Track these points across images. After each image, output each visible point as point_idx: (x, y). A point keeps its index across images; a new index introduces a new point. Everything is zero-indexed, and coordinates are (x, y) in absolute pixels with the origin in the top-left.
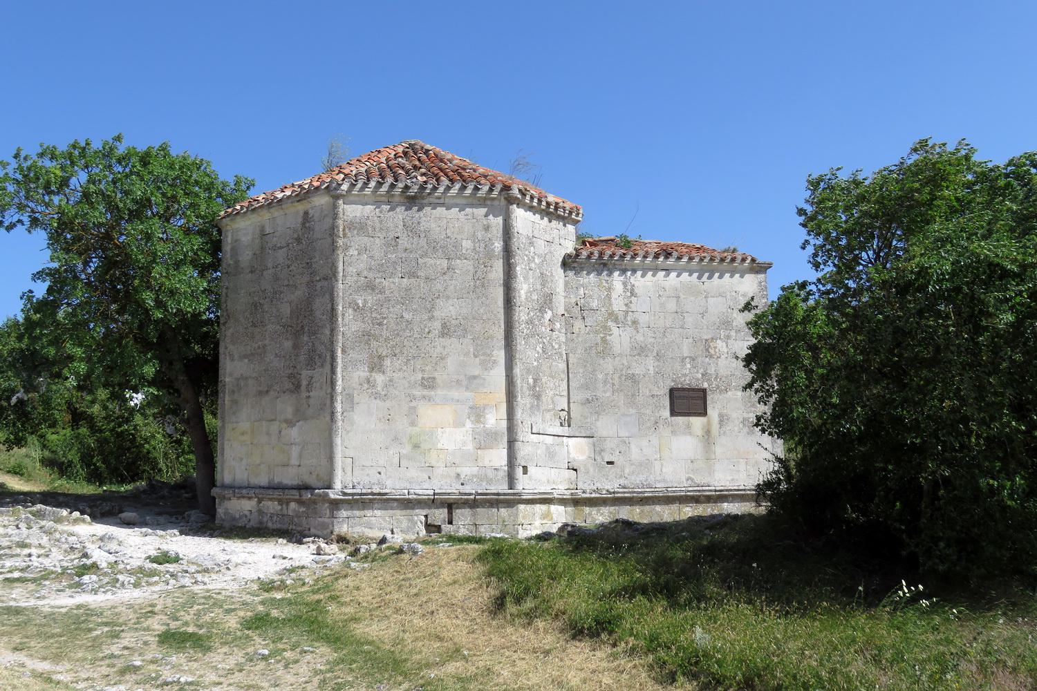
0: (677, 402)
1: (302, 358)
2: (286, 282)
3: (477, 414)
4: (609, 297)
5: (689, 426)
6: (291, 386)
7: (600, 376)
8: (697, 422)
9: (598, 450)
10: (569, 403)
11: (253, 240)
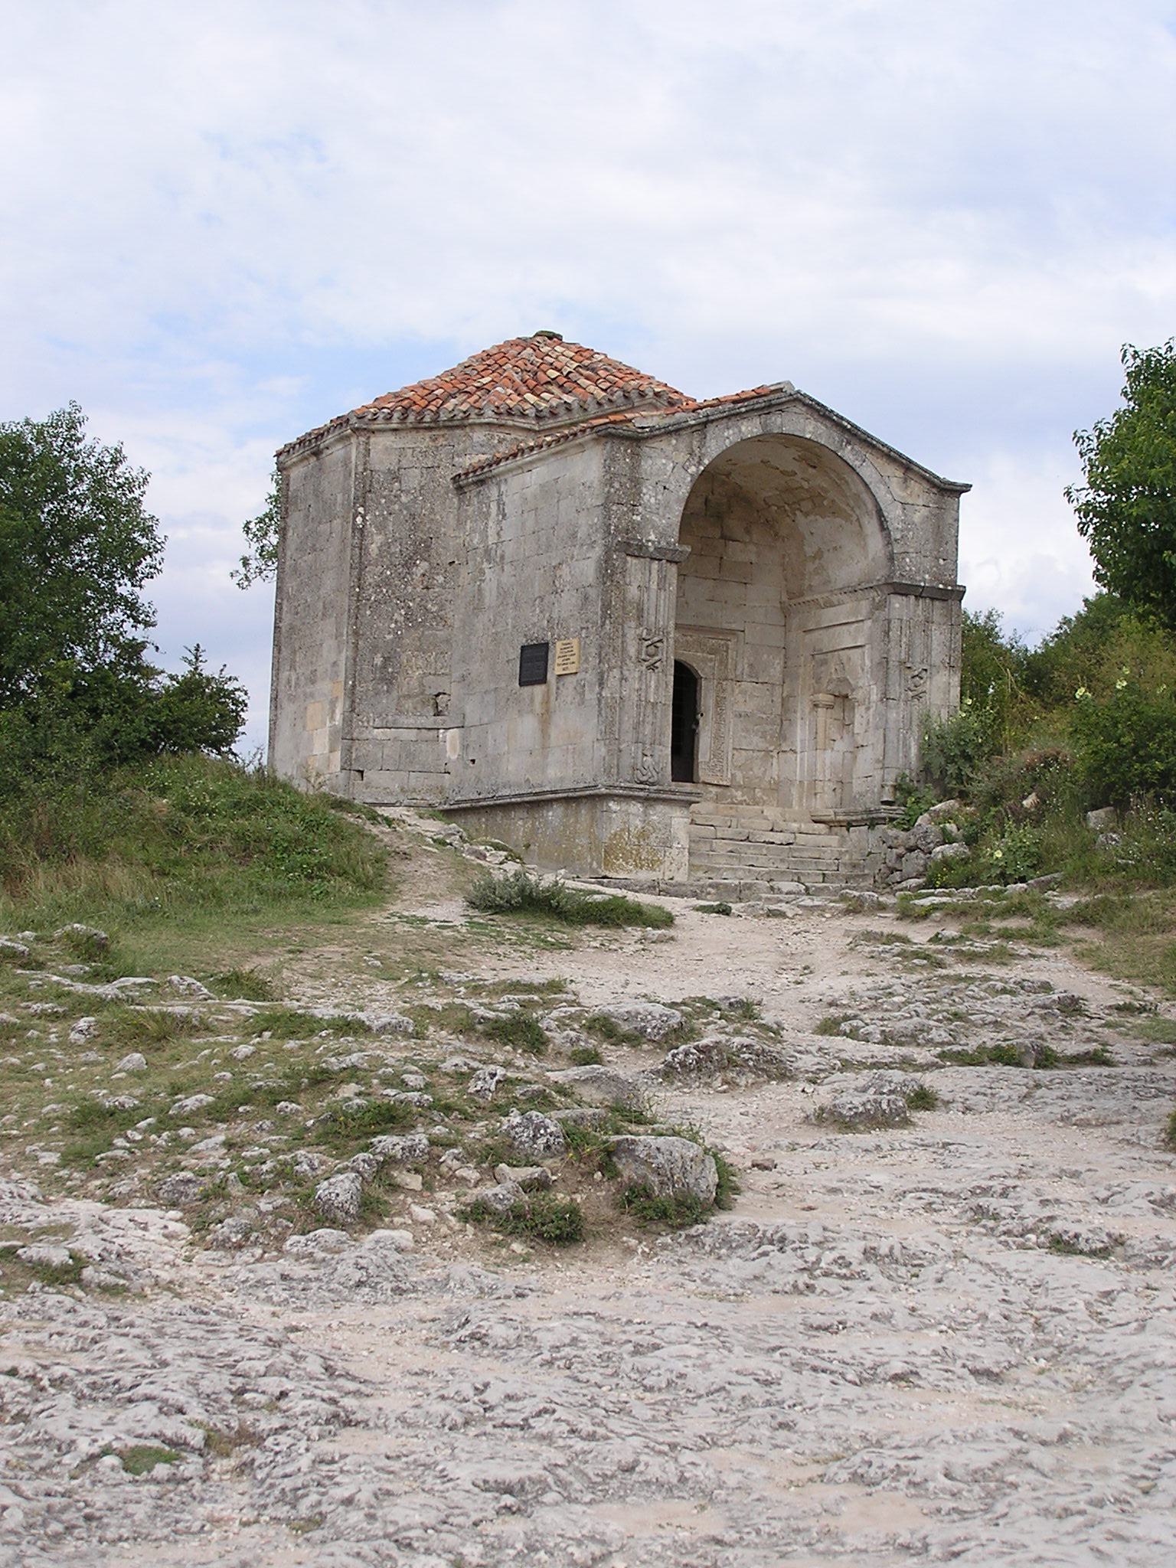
5: (532, 700)
8: (539, 690)
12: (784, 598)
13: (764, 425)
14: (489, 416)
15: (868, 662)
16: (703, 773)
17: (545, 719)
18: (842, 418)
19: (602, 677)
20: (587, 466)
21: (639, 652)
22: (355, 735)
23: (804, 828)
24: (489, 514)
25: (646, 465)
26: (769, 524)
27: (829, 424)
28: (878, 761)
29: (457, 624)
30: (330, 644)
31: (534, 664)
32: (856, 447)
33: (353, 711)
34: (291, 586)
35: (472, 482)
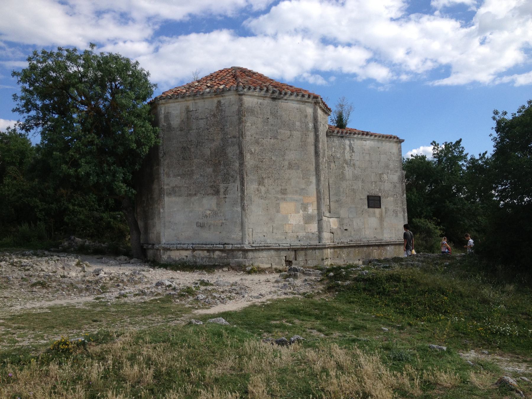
0: (370, 202)
1: (220, 177)
2: (206, 137)
3: (305, 207)
4: (344, 153)
5: (374, 213)
6: (212, 192)
7: (341, 190)
8: (377, 211)
9: (341, 224)
10: (330, 202)
11: (181, 113)
17: (381, 219)
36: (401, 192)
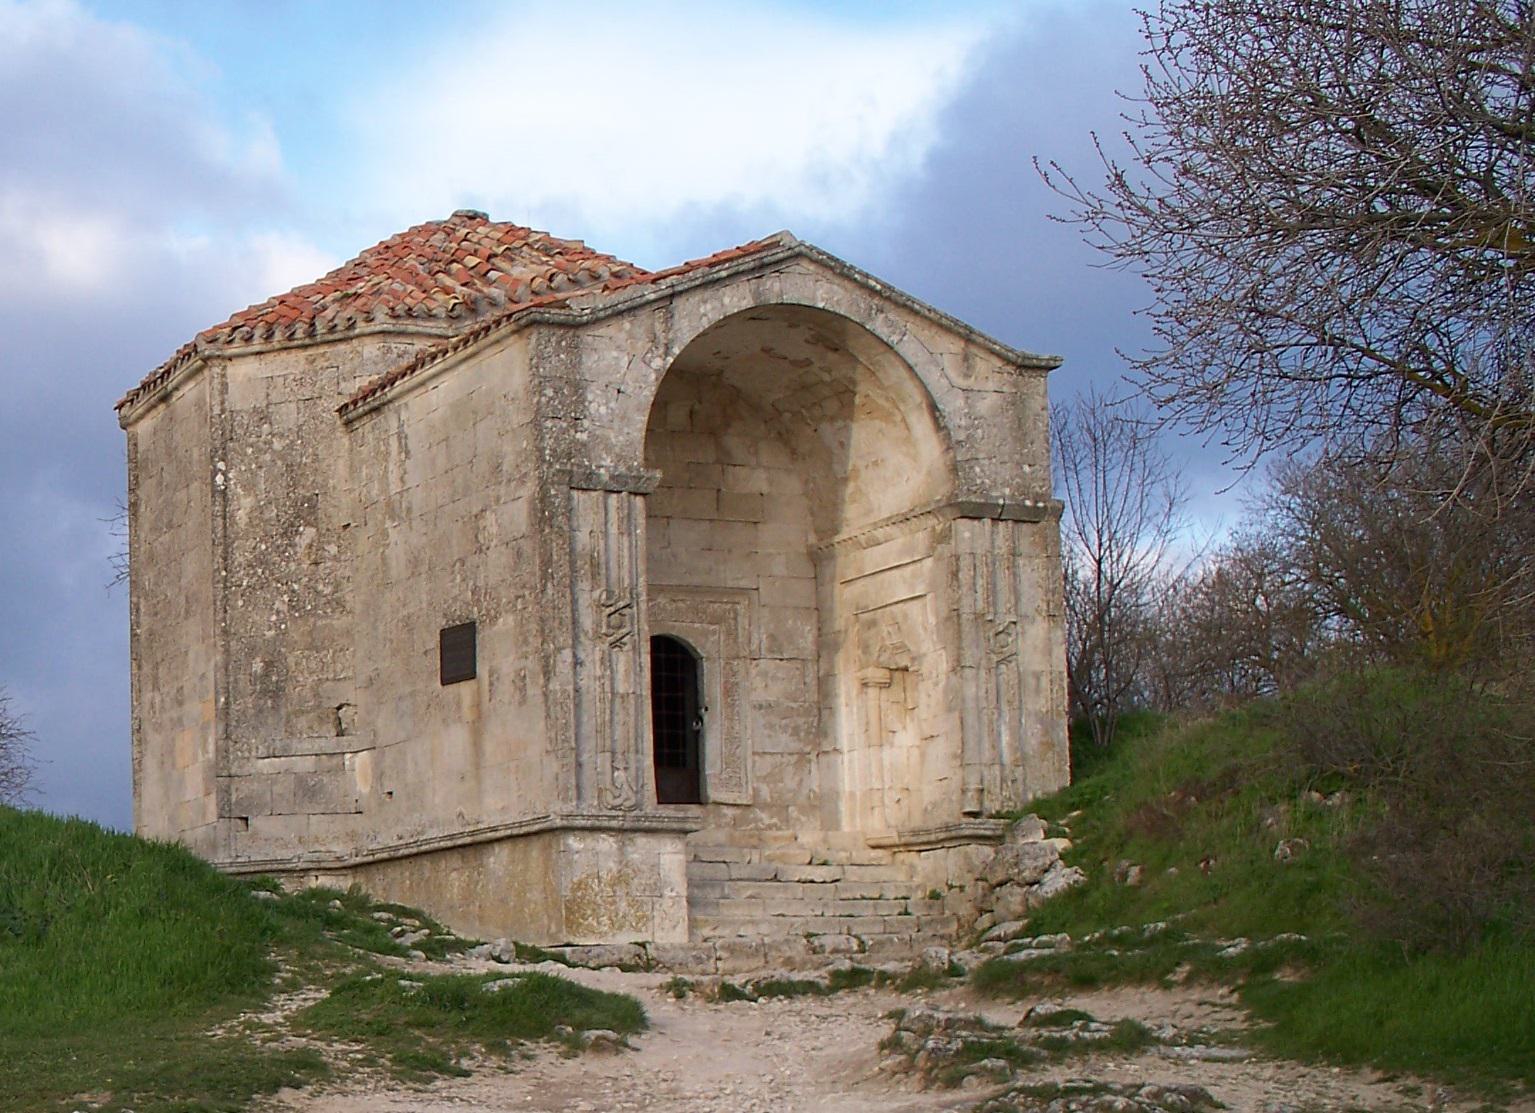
8: (465, 689)
12: (812, 539)
13: (756, 294)
14: (382, 321)
15: (932, 620)
16: (713, 793)
18: (867, 276)
19: (547, 665)
20: (506, 367)
21: (599, 625)
22: (233, 772)
23: (857, 857)
24: (388, 453)
25: (589, 361)
26: (784, 439)
27: (849, 285)
28: (955, 756)
29: (358, 608)
30: (196, 649)
31: (458, 653)
32: (891, 316)
33: (228, 737)
34: (148, 579)
35: (364, 408)
36: (536, 581)
